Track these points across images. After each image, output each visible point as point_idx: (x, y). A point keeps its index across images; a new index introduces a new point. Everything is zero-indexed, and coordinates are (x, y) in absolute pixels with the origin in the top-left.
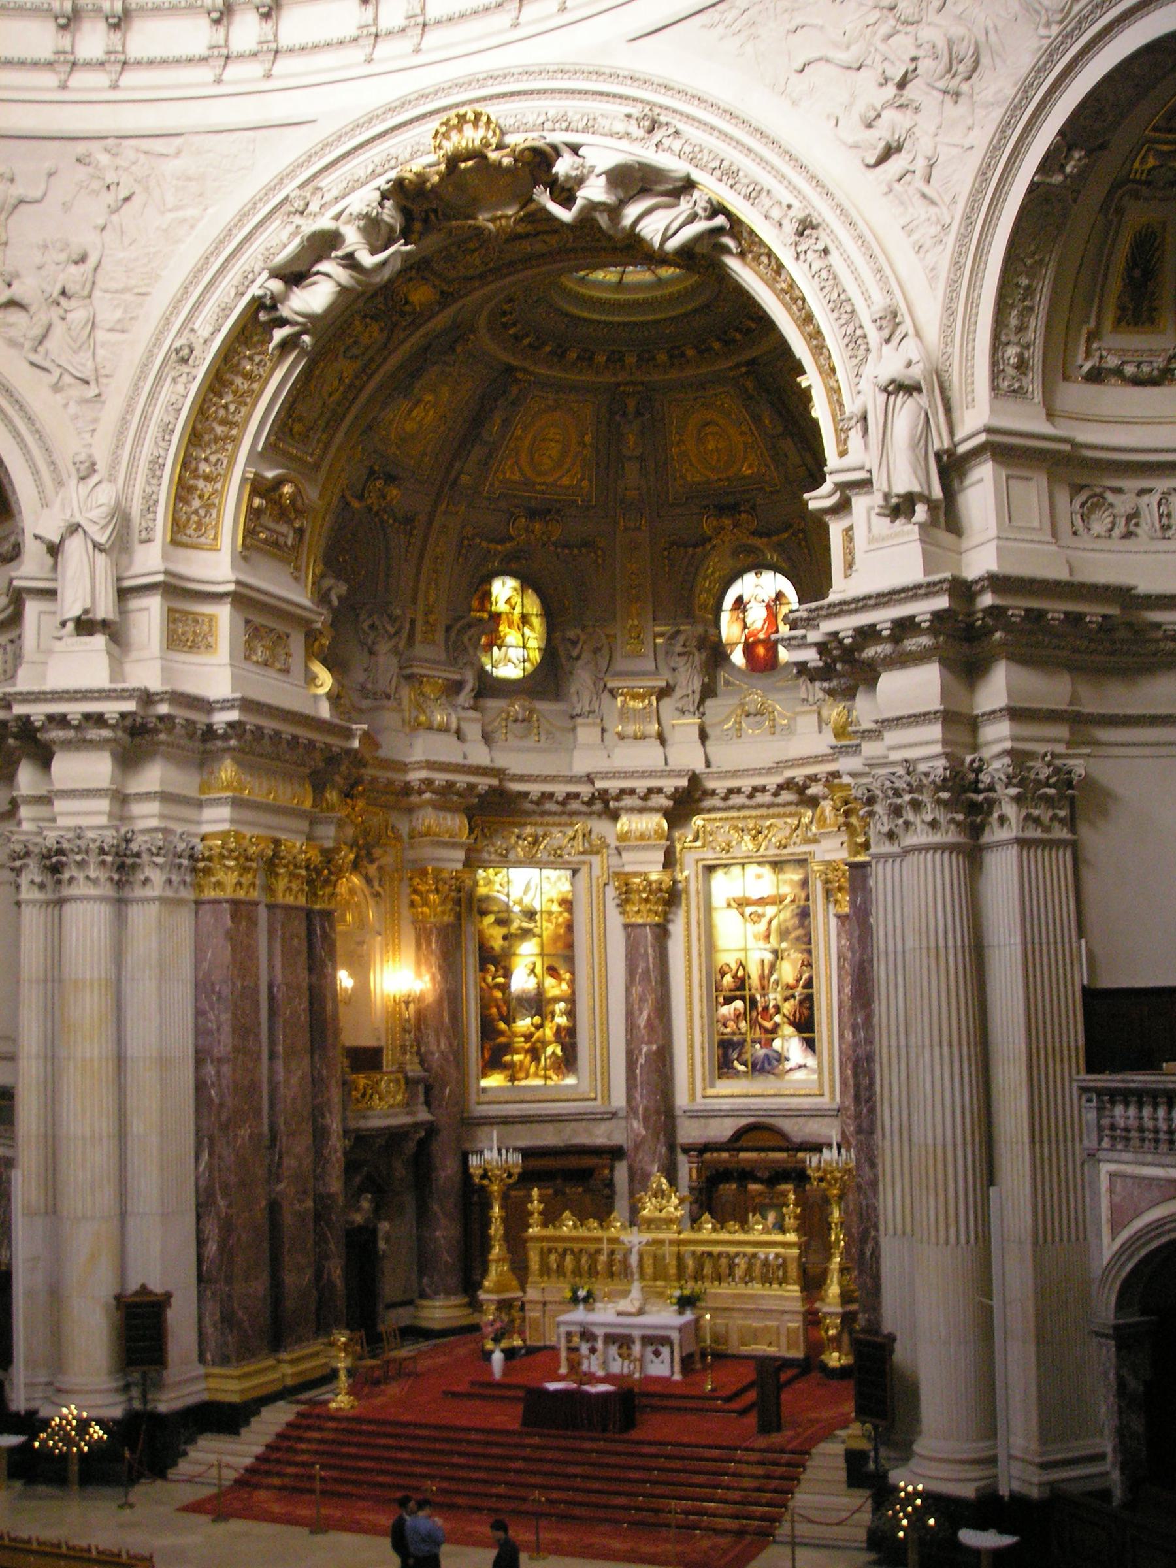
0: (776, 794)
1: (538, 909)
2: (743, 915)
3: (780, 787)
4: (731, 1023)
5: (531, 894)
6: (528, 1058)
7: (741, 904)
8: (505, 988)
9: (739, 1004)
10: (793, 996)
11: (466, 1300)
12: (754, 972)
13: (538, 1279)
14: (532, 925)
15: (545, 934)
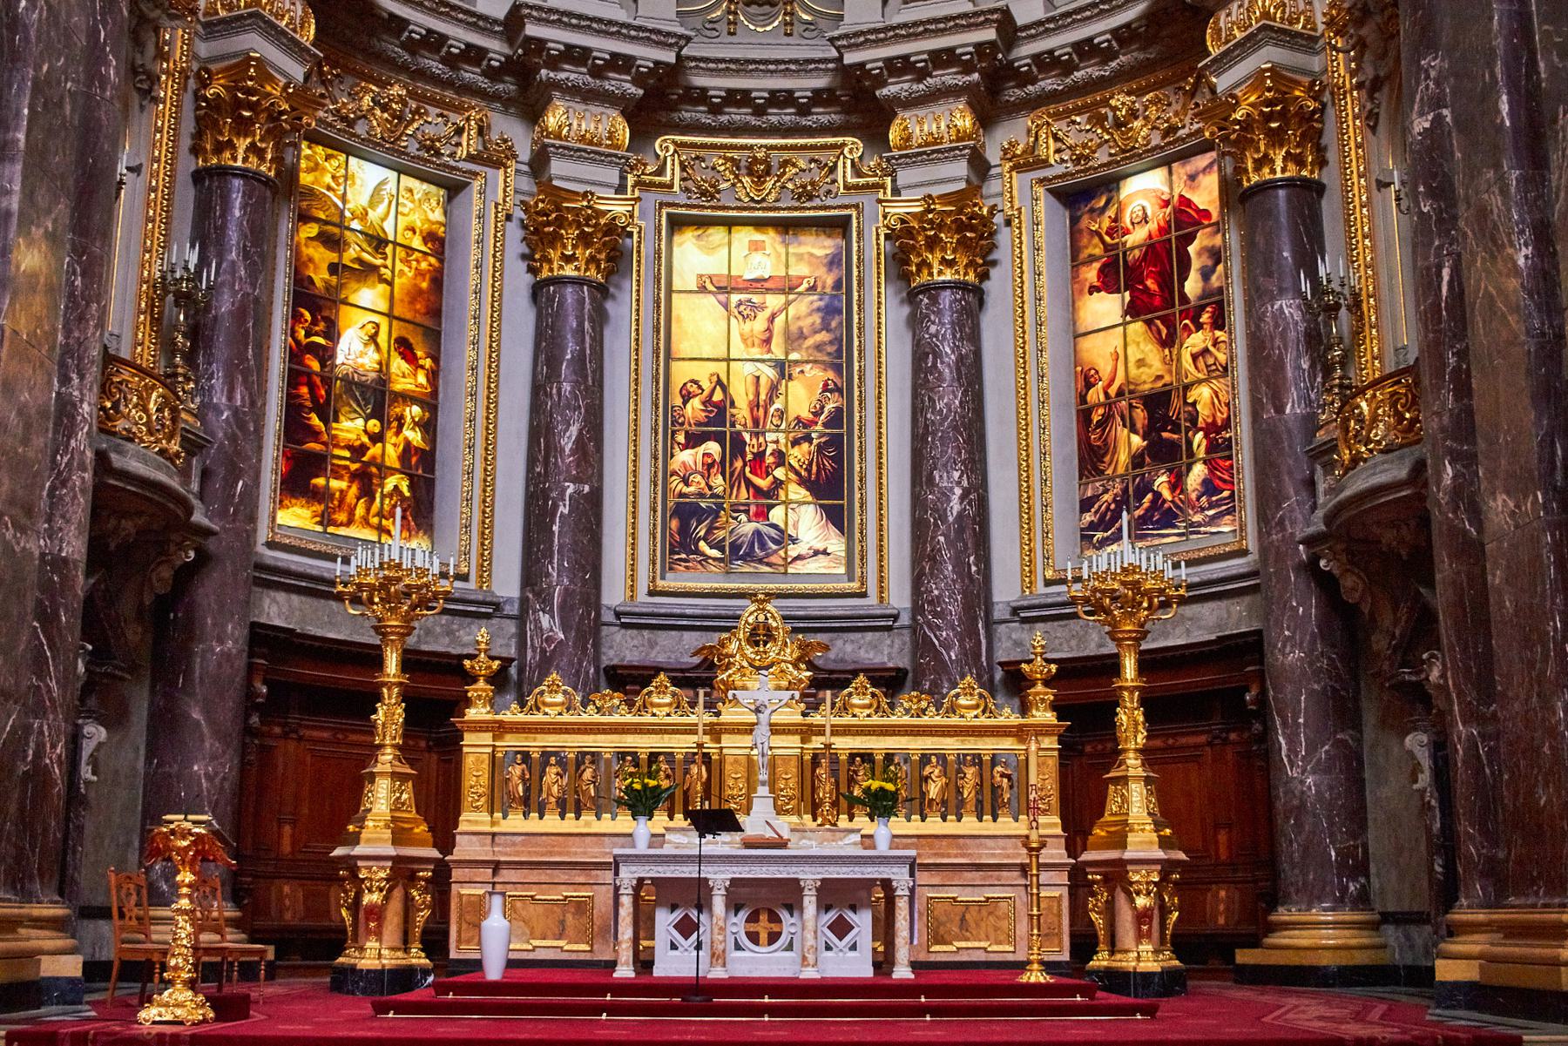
0: (804, 111)
1: (391, 238)
2: (726, 306)
3: (818, 97)
4: (699, 478)
5: (382, 209)
6: (354, 490)
7: (724, 287)
8: (326, 355)
9: (713, 447)
10: (808, 439)
11: (238, 914)
12: (741, 395)
13: (485, 817)
14: (379, 262)
15: (397, 280)
